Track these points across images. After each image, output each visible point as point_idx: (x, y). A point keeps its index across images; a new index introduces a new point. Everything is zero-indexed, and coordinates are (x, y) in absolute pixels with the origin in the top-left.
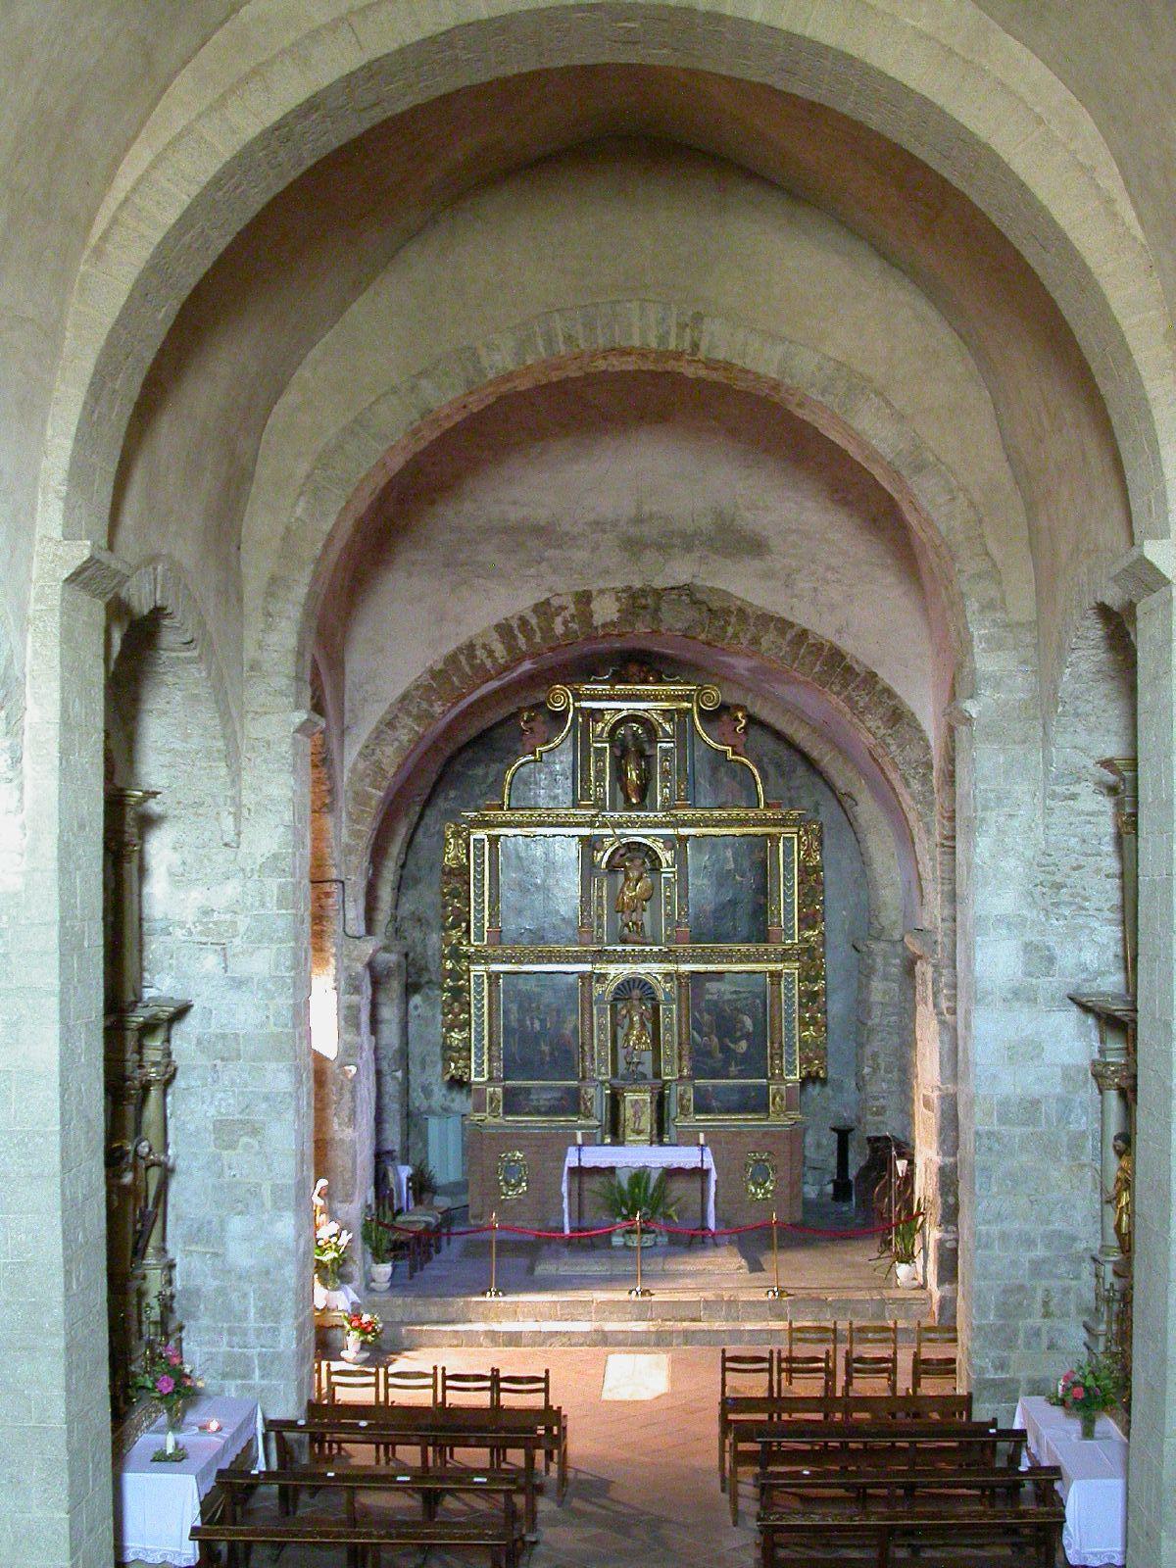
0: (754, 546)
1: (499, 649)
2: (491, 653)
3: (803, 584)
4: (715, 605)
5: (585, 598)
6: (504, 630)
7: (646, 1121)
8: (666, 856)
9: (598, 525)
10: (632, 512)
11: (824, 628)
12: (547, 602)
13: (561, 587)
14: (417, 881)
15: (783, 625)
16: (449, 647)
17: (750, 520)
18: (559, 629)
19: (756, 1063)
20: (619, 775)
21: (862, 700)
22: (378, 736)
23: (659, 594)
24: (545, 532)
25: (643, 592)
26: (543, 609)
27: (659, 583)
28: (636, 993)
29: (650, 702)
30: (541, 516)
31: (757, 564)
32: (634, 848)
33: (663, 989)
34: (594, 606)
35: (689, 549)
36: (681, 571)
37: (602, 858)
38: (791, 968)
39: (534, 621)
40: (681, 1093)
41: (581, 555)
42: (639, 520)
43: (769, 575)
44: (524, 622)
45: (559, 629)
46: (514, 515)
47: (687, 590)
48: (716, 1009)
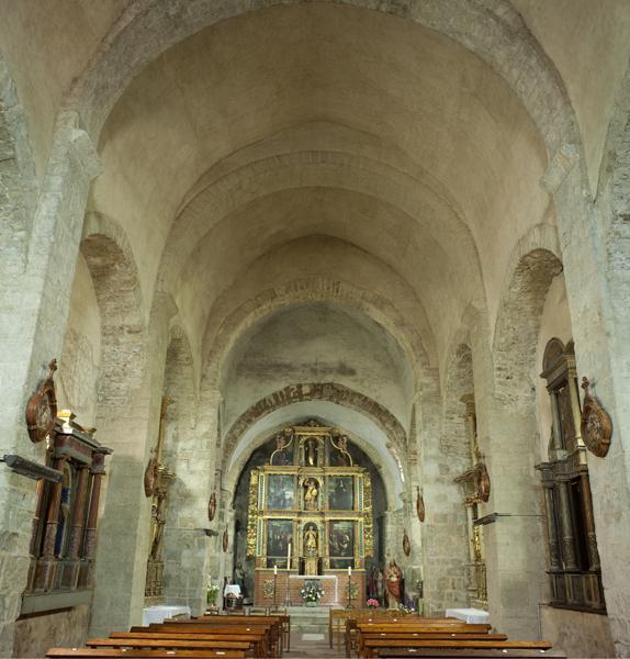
0: (352, 372)
1: (273, 401)
2: (271, 402)
3: (366, 384)
4: (340, 389)
5: (300, 386)
6: (275, 395)
7: (315, 569)
8: (321, 483)
9: (304, 365)
10: (314, 361)
11: (372, 396)
12: (288, 387)
13: (293, 383)
14: (240, 494)
15: (360, 395)
16: (258, 400)
17: (350, 365)
18: (292, 395)
19: (351, 551)
20: (307, 459)
21: (384, 418)
22: (234, 427)
23: (323, 385)
24: (290, 367)
25: (319, 385)
26: (287, 389)
27: (322, 382)
28: (311, 528)
29: (317, 432)
30: (287, 362)
31: (351, 378)
32: (311, 479)
33: (319, 526)
34: (303, 388)
35: (331, 372)
36: (329, 379)
37: (301, 483)
38: (361, 519)
39: (284, 393)
40: (327, 561)
41: (299, 373)
42: (316, 364)
43: (355, 381)
44: (281, 393)
45: (292, 395)
46: (279, 362)
47: (331, 384)
48: (337, 532)
